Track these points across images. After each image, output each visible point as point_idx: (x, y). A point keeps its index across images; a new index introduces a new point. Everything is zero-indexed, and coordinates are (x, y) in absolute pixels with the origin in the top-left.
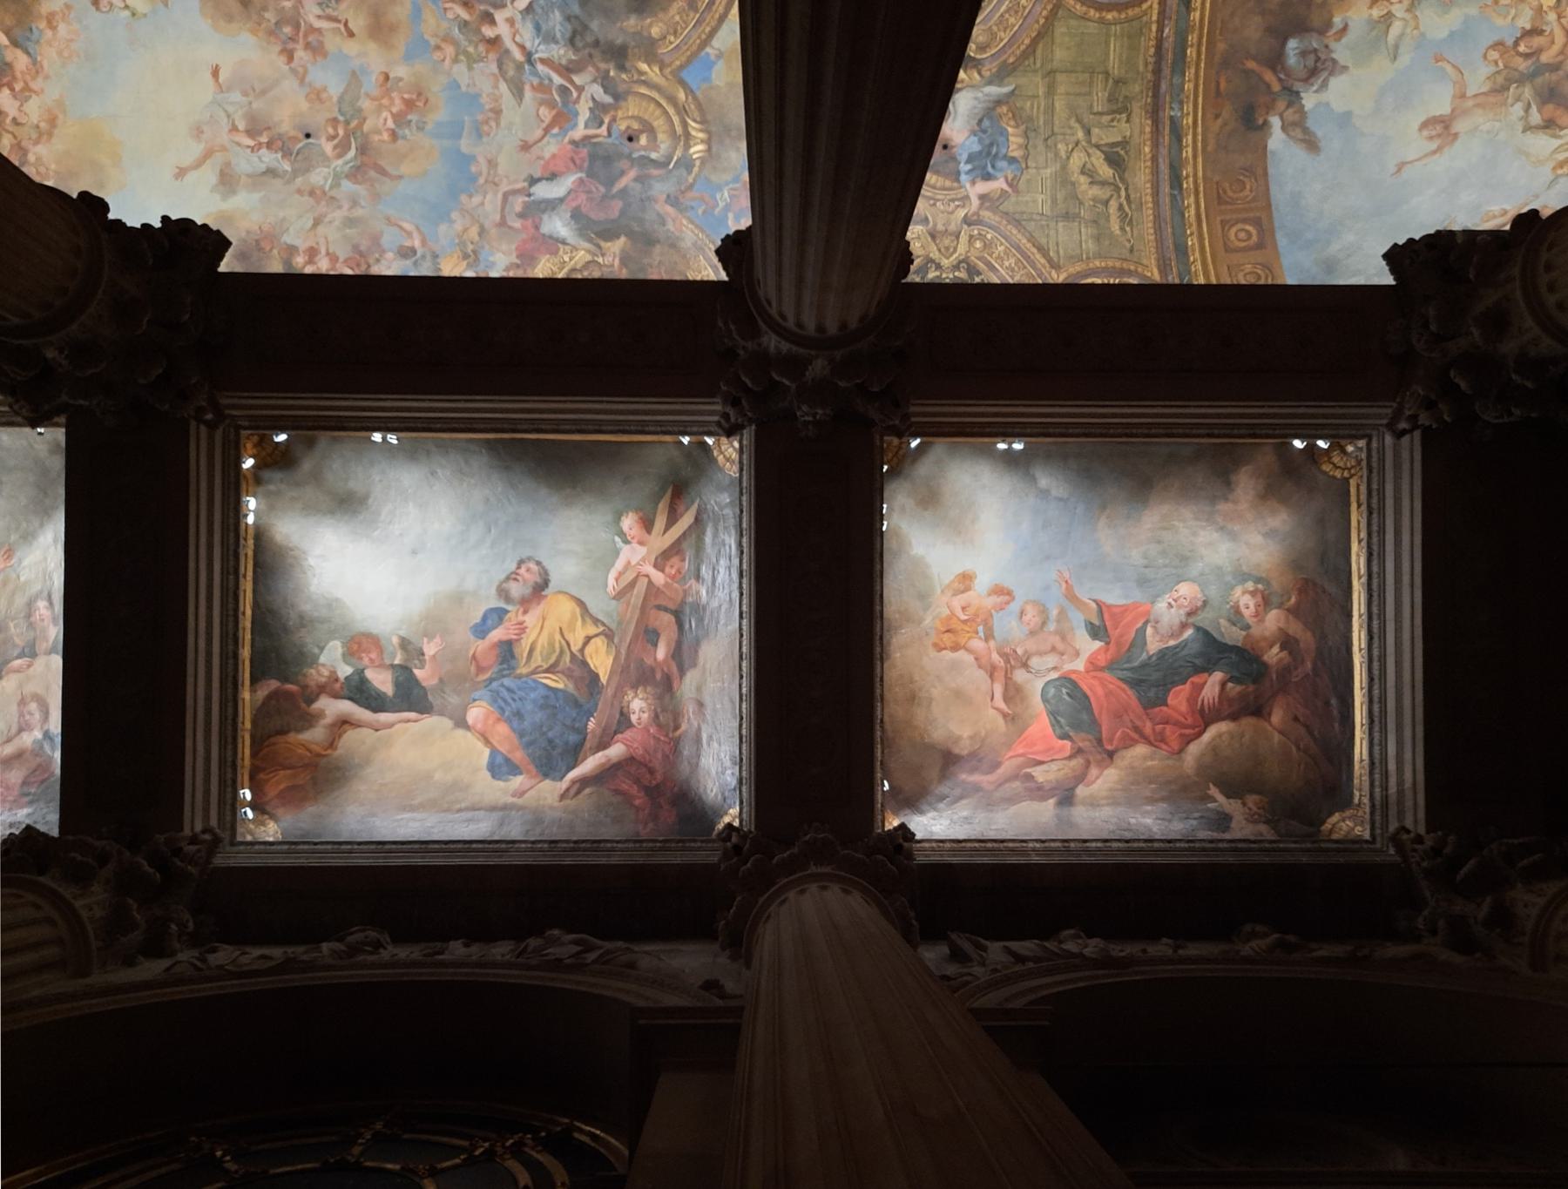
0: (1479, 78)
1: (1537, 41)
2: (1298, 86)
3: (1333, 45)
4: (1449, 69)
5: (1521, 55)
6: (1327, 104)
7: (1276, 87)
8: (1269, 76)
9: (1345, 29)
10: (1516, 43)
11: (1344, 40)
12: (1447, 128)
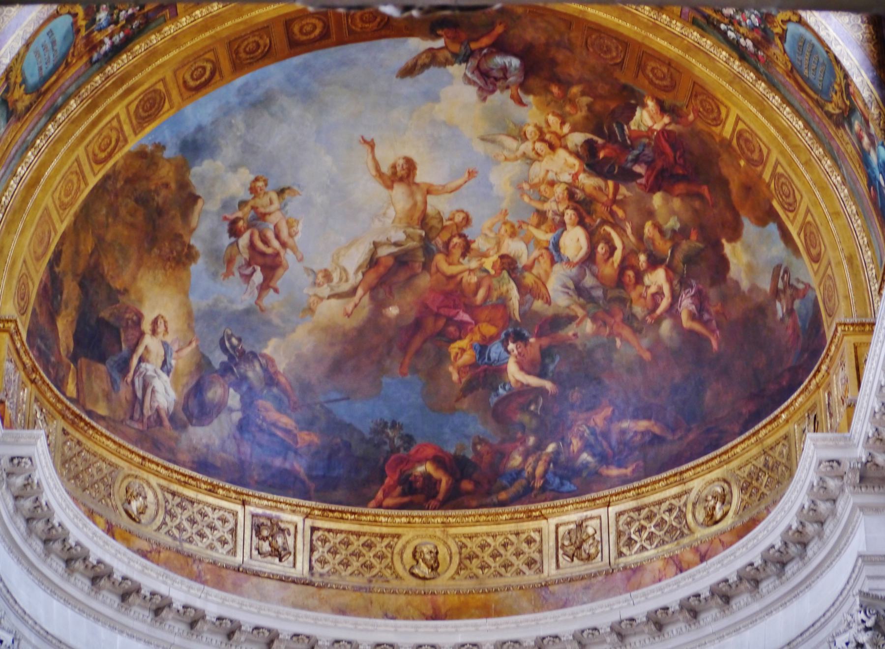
0: (440, 205)
1: (457, 252)
2: (473, 62)
3: (508, 93)
4: (460, 181)
5: (450, 240)
6: (450, 83)
7: (474, 46)
8: (486, 41)
9: (520, 103)
10: (462, 236)
11: (511, 102)
12: (401, 180)
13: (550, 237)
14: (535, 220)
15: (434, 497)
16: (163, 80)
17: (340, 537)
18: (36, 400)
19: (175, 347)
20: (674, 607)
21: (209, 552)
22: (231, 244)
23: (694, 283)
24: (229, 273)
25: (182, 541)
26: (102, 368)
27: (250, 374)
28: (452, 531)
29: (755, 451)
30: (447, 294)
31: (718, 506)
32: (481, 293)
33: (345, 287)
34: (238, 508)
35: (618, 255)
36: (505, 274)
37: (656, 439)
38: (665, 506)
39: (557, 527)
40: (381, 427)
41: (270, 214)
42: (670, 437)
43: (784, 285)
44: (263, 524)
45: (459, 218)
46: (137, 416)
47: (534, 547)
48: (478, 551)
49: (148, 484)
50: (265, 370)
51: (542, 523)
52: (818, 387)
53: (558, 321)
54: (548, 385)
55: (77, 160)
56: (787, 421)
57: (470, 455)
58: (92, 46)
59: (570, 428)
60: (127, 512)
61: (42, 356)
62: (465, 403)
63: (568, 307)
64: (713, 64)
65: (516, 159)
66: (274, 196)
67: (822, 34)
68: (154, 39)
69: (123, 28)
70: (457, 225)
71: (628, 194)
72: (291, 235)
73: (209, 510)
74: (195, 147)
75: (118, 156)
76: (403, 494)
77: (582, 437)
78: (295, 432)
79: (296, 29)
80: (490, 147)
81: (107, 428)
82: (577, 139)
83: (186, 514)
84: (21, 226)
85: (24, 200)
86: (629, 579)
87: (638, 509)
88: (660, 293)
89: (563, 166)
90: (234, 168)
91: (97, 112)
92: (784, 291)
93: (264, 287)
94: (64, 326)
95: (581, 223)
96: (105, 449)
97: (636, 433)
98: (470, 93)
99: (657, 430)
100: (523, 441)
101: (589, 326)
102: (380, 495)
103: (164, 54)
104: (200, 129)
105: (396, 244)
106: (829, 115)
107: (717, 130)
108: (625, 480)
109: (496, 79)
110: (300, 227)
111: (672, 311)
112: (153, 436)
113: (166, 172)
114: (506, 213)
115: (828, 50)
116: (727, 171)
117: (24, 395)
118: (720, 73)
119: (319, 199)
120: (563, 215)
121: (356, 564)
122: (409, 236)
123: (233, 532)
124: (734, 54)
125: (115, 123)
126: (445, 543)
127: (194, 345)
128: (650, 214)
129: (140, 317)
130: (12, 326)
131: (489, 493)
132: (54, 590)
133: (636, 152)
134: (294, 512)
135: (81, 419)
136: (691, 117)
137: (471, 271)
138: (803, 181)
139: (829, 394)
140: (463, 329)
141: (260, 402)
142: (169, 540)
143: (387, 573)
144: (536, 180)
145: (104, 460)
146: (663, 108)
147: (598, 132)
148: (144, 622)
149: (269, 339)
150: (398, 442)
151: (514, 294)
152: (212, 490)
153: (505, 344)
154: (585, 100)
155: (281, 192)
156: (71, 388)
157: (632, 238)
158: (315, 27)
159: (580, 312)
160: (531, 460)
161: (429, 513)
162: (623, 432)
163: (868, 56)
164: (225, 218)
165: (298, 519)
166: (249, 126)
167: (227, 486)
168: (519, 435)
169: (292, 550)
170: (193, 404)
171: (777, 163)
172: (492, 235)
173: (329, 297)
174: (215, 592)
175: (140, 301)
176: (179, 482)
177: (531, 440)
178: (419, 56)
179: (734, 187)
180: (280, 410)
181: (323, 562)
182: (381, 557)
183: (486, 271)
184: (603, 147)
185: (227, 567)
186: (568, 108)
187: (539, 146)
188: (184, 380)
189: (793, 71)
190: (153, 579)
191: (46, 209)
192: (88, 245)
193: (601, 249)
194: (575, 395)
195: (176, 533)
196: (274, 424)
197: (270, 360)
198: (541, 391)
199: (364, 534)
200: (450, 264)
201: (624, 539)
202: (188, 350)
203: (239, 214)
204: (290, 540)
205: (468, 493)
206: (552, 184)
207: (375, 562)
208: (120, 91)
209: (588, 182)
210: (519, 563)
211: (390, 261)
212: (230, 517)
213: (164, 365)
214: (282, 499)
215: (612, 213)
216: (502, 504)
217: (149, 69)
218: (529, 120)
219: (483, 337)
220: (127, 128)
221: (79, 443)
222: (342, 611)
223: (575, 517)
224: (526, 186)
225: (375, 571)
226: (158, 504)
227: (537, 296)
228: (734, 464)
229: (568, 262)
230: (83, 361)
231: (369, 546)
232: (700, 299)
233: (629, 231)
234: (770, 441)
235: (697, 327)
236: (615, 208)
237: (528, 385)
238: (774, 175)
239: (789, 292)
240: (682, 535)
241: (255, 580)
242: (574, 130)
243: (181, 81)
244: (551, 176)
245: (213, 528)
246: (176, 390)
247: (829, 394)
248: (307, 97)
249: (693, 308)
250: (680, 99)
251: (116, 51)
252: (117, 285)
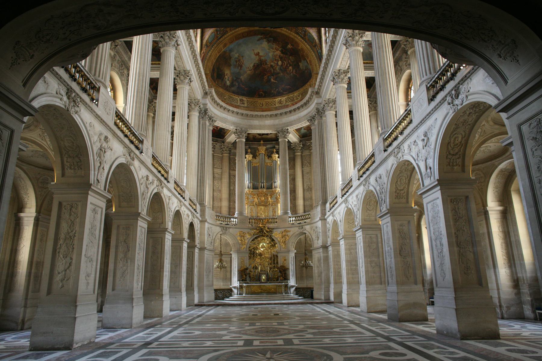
0: (263, 58)
61: (213, 79)
64: (298, 39)
82: (280, 49)
89: (278, 53)
93: (240, 69)
96: (221, 90)
128: (290, 59)
132: (216, 108)
209: (282, 55)
222: (251, 111)
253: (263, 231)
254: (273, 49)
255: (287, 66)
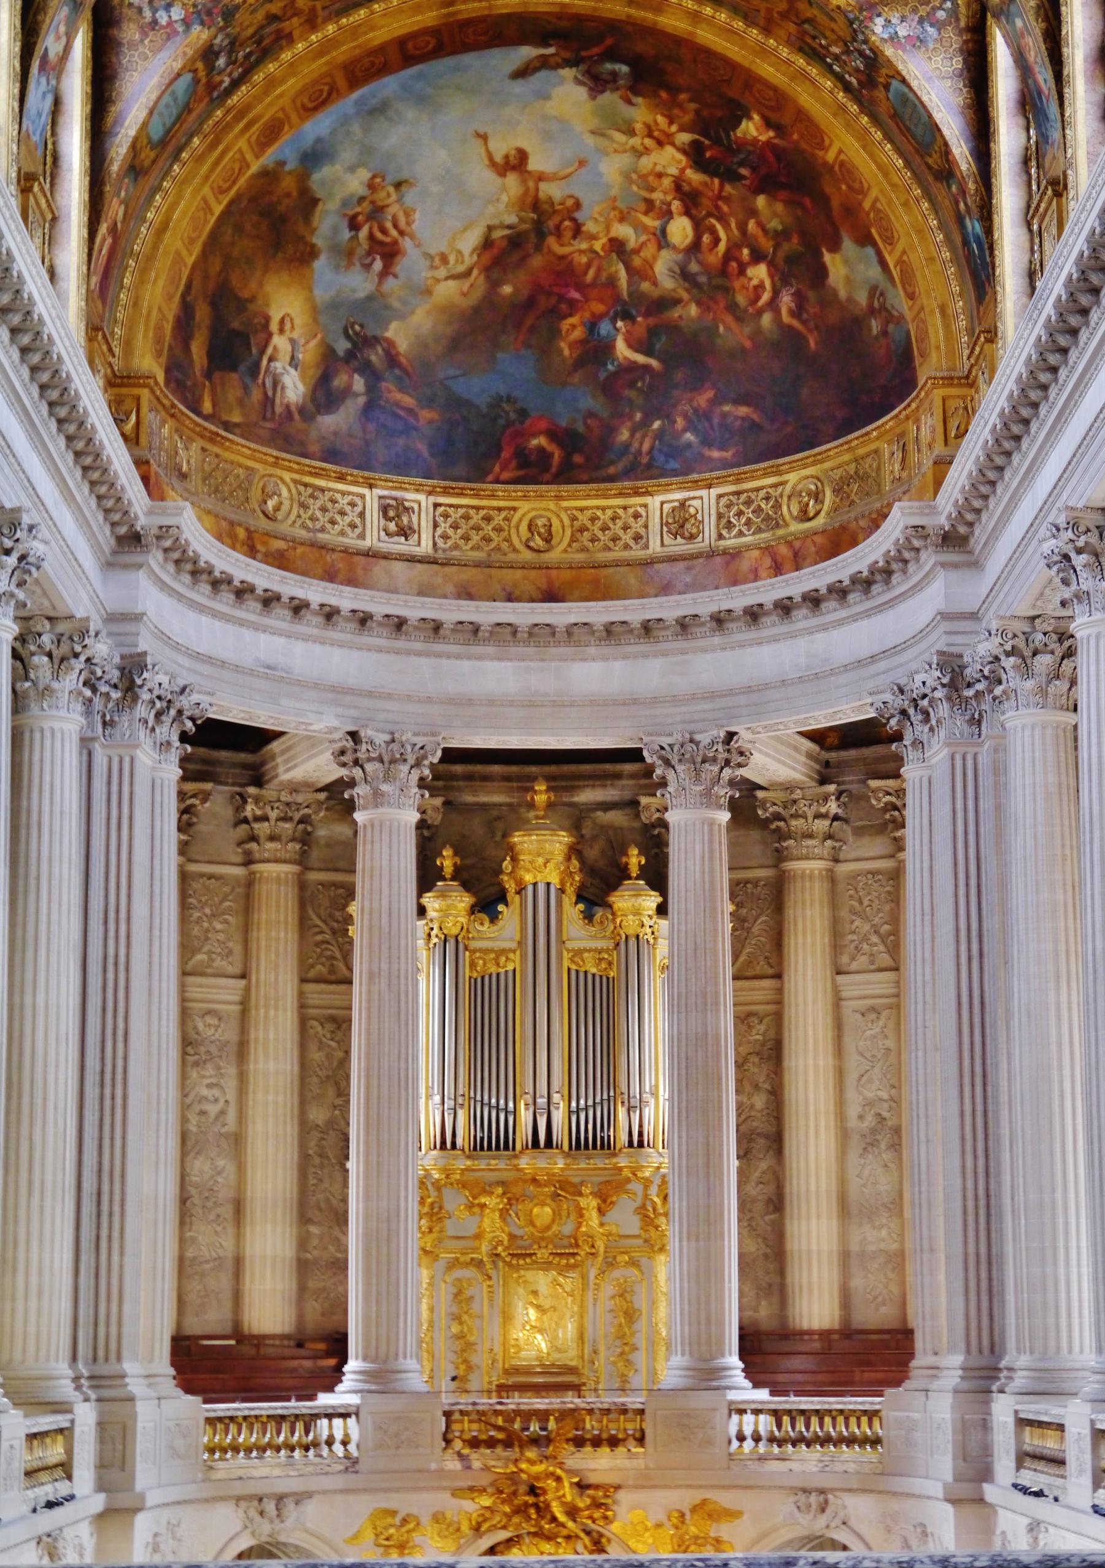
0: (552, 191)
1: (568, 234)
3: (619, 93)
4: (569, 170)
5: (561, 222)
6: (561, 83)
7: (584, 54)
9: (630, 102)
10: (574, 220)
12: (514, 168)
13: (657, 223)
14: (642, 206)
15: (547, 469)
16: (283, 109)
17: (461, 511)
18: (177, 430)
19: (302, 341)
20: (769, 606)
21: (341, 539)
22: (352, 238)
23: (794, 282)
24: (350, 264)
25: (315, 531)
26: (234, 376)
27: (373, 358)
28: (565, 504)
29: (847, 457)
30: (558, 274)
31: (812, 503)
32: (591, 273)
33: (461, 269)
34: (366, 491)
35: (722, 246)
36: (614, 256)
37: (755, 427)
38: (762, 494)
39: (662, 503)
40: (498, 401)
41: (387, 206)
42: (768, 426)
43: (878, 306)
44: (389, 505)
45: (570, 203)
46: (268, 415)
47: (641, 521)
48: (588, 524)
49: (282, 479)
50: (387, 353)
51: (648, 500)
52: (907, 418)
53: (665, 303)
54: (654, 363)
55: (204, 199)
56: (877, 438)
57: (581, 428)
58: (211, 87)
59: (675, 406)
60: (264, 513)
62: (577, 378)
63: (674, 290)
65: (625, 151)
66: (391, 189)
67: (925, 99)
68: (271, 67)
69: (241, 65)
70: (570, 210)
71: (733, 192)
72: (408, 224)
73: (338, 496)
74: (314, 157)
75: (242, 181)
76: (520, 467)
77: (685, 416)
78: (417, 410)
79: (410, 45)
80: (600, 140)
81: (242, 436)
82: (684, 138)
83: (319, 503)
84: (153, 274)
85: (155, 247)
86: (727, 564)
87: (738, 493)
88: (760, 287)
89: (670, 160)
90: (352, 169)
91: (221, 148)
92: (880, 311)
93: (385, 273)
94: (198, 349)
95: (687, 213)
97: (736, 418)
98: (581, 93)
99: (755, 417)
100: (631, 417)
101: (693, 310)
102: (497, 469)
103: (283, 81)
104: (319, 140)
105: (509, 227)
106: (929, 167)
107: (821, 153)
108: (726, 465)
109: (606, 82)
110: (417, 216)
111: (773, 304)
112: (283, 432)
113: (288, 184)
114: (615, 199)
115: (930, 116)
116: (828, 188)
117: (165, 431)
118: (824, 104)
119: (436, 189)
120: (669, 204)
121: (476, 538)
122: (522, 220)
123: (362, 515)
124: (839, 85)
125: (238, 156)
126: (558, 516)
127: (319, 336)
128: (754, 213)
129: (268, 319)
130: (151, 381)
131: (597, 468)
133: (742, 156)
134: (417, 490)
135: (218, 434)
136: (795, 137)
137: (581, 252)
138: (902, 220)
139: (918, 429)
140: (573, 307)
141: (384, 384)
142: (303, 533)
143: (505, 546)
144: (644, 172)
145: (240, 465)
146: (768, 124)
147: (705, 133)
148: (284, 620)
149: (388, 323)
150: (513, 416)
151: (623, 274)
152: (341, 478)
153: (614, 322)
154: (693, 106)
155: (398, 185)
156: (207, 407)
157: (736, 232)
158: (428, 43)
159: (685, 296)
160: (638, 435)
161: (543, 487)
162: (724, 415)
163: (968, 124)
164: (345, 215)
165: (421, 497)
166: (366, 130)
167: (355, 472)
168: (627, 410)
169: (416, 527)
170: (320, 395)
171: (876, 200)
172: (601, 219)
173: (447, 278)
174: (348, 589)
175: (267, 305)
176: (311, 474)
177: (638, 416)
178: (531, 61)
179: (835, 203)
180: (402, 390)
181: (445, 537)
182: (498, 530)
183: (596, 252)
184: (709, 148)
185: (359, 553)
186: (676, 111)
187: (648, 141)
188: (311, 372)
189: (895, 116)
190: (290, 585)
191: (177, 252)
192: (216, 266)
193: (706, 239)
194: (679, 375)
195: (309, 524)
196: (397, 404)
197: (391, 343)
198: (646, 368)
199: (483, 508)
200: (562, 245)
201: (724, 521)
202: (314, 343)
203: (358, 209)
204: (415, 518)
205: (579, 466)
206: (660, 175)
207: (493, 535)
208: (241, 125)
209: (694, 177)
210: (627, 537)
211: (504, 244)
212: (358, 500)
213: (293, 362)
214: (406, 479)
215: (717, 208)
216: (612, 479)
217: (268, 100)
218: (639, 118)
219: (593, 315)
220: (249, 156)
221: (217, 456)
223: (679, 496)
224: (634, 177)
225: (493, 545)
226: (291, 499)
227: (645, 277)
228: (828, 465)
229: (674, 248)
230: (217, 375)
231: (488, 519)
232: (799, 297)
233: (733, 225)
234: (861, 451)
235: (796, 323)
236: (720, 203)
237: (635, 362)
238: (873, 207)
239: (884, 314)
240: (778, 525)
241: (383, 563)
242: (682, 129)
243: (299, 103)
244: (659, 168)
245: (343, 513)
246: (304, 383)
247: (918, 429)
248: (421, 100)
249: (793, 305)
250: (787, 119)
251: (235, 84)
252: (245, 294)
253: (543, 1510)
254: (631, 133)
255: (728, 257)
